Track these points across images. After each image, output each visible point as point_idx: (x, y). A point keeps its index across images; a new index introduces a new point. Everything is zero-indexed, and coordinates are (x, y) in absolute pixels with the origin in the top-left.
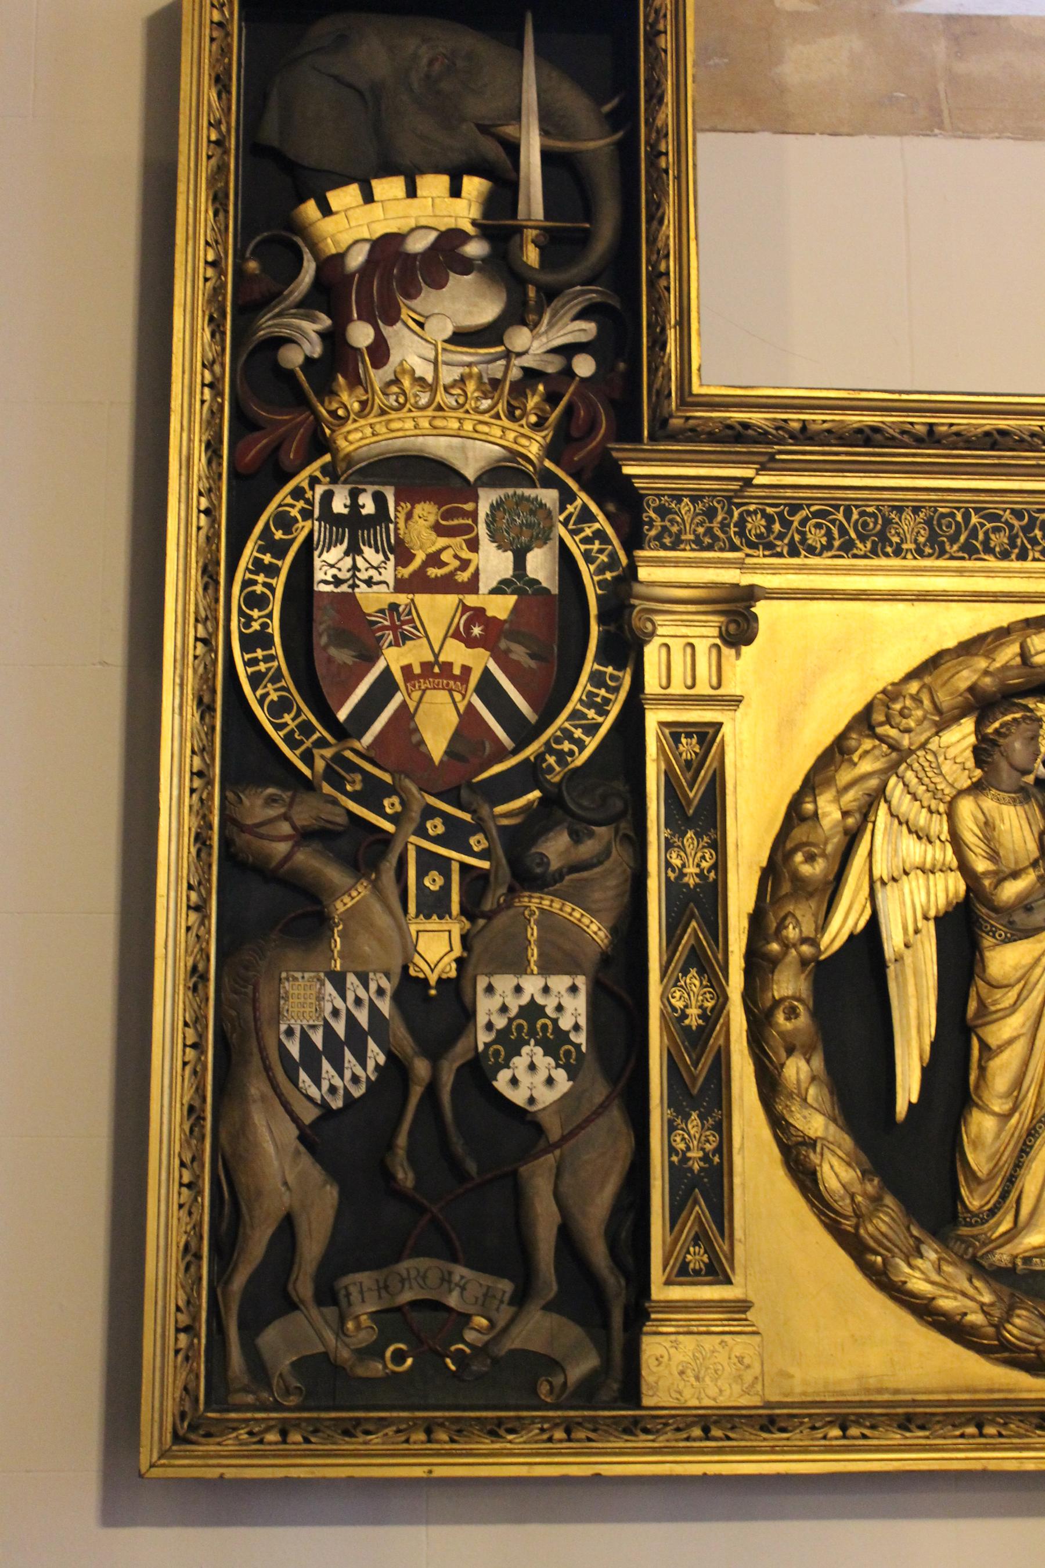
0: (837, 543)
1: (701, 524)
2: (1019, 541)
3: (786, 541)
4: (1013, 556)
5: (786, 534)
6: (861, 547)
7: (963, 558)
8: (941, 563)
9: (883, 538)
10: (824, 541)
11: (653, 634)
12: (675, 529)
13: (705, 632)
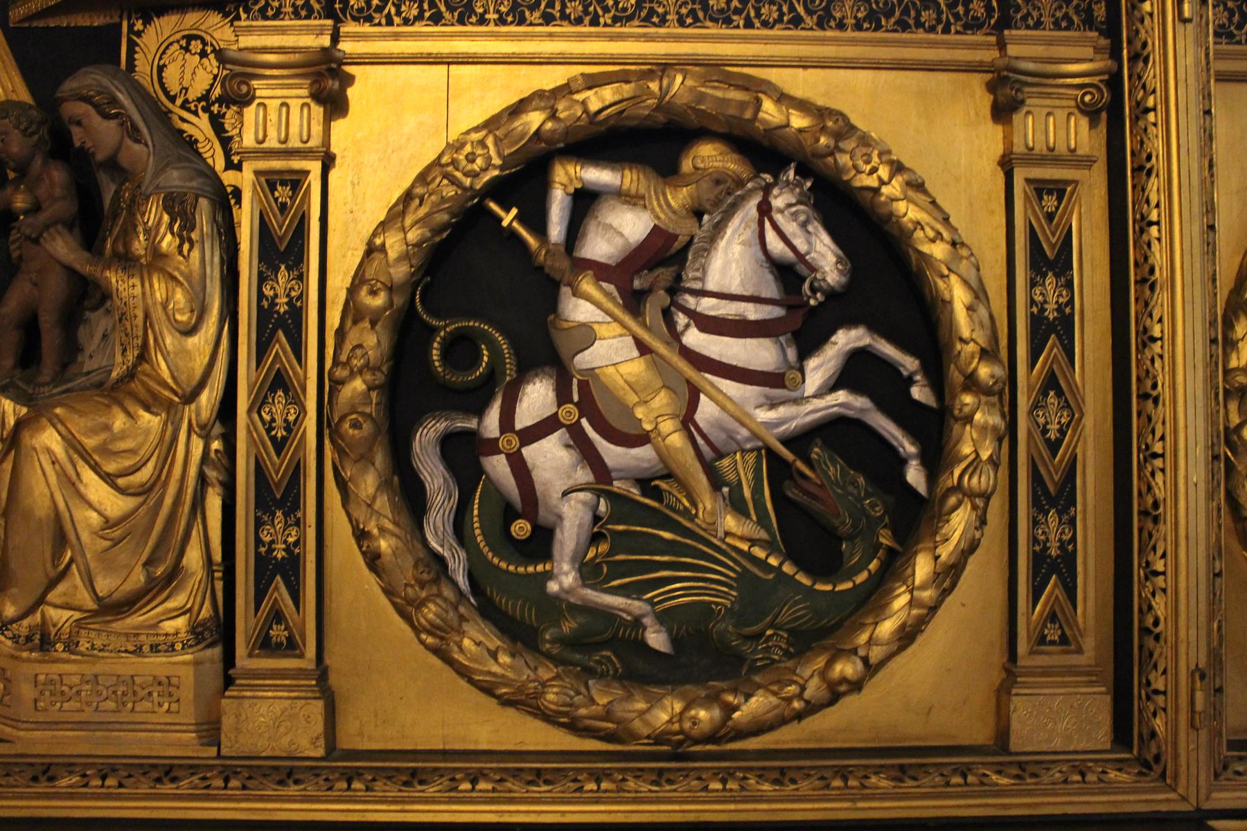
6: (809, 21)
11: (254, 98)
13: (297, 96)
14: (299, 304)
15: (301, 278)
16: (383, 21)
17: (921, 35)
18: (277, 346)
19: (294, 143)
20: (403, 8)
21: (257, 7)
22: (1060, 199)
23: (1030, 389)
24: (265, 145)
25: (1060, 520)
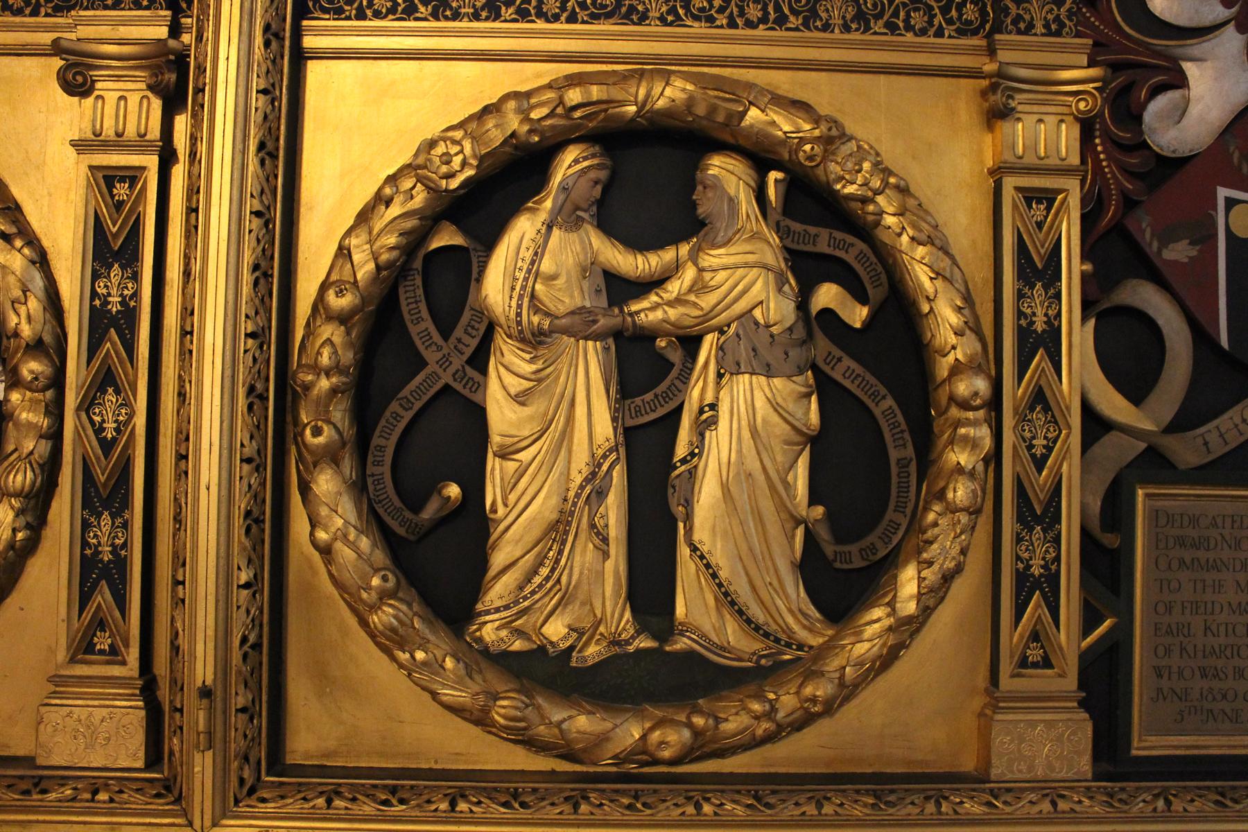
3: (726, 14)
4: (563, 19)
5: (726, 8)
7: (404, 19)
8: (497, 25)
9: (816, 15)
15: (136, 277)
17: (541, 25)
18: (108, 344)
22: (131, 187)
23: (79, 388)
25: (113, 523)
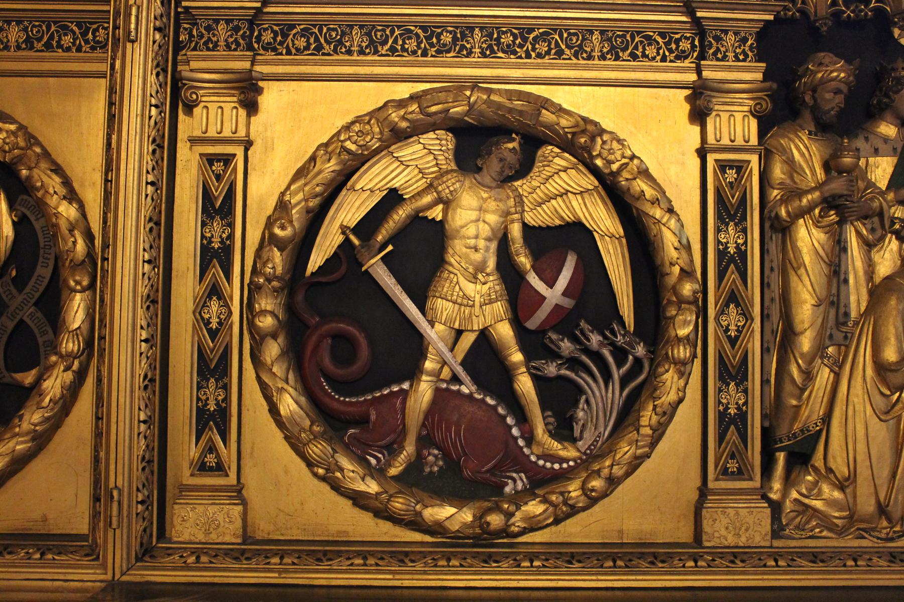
0: (313, 46)
1: (485, 41)
2: (78, 42)
10: (406, 46)
12: (214, 39)
14: (743, 248)
16: (523, 56)
19: (739, 142)
20: (537, 46)
21: (711, 51)
24: (721, 142)
